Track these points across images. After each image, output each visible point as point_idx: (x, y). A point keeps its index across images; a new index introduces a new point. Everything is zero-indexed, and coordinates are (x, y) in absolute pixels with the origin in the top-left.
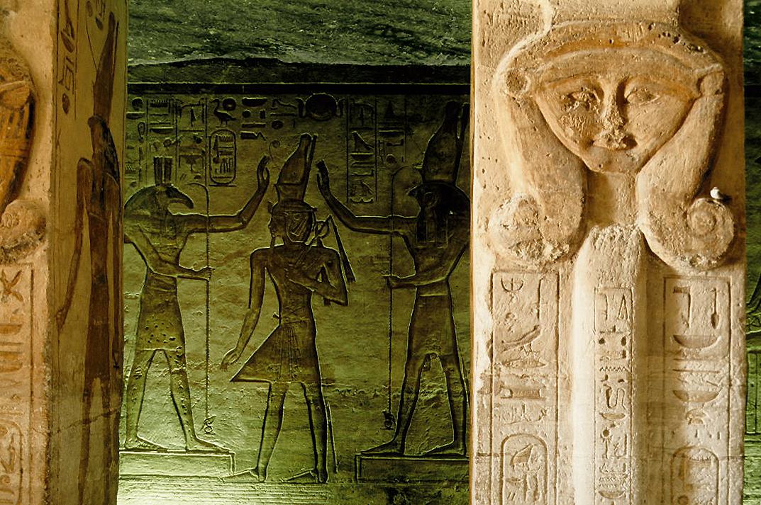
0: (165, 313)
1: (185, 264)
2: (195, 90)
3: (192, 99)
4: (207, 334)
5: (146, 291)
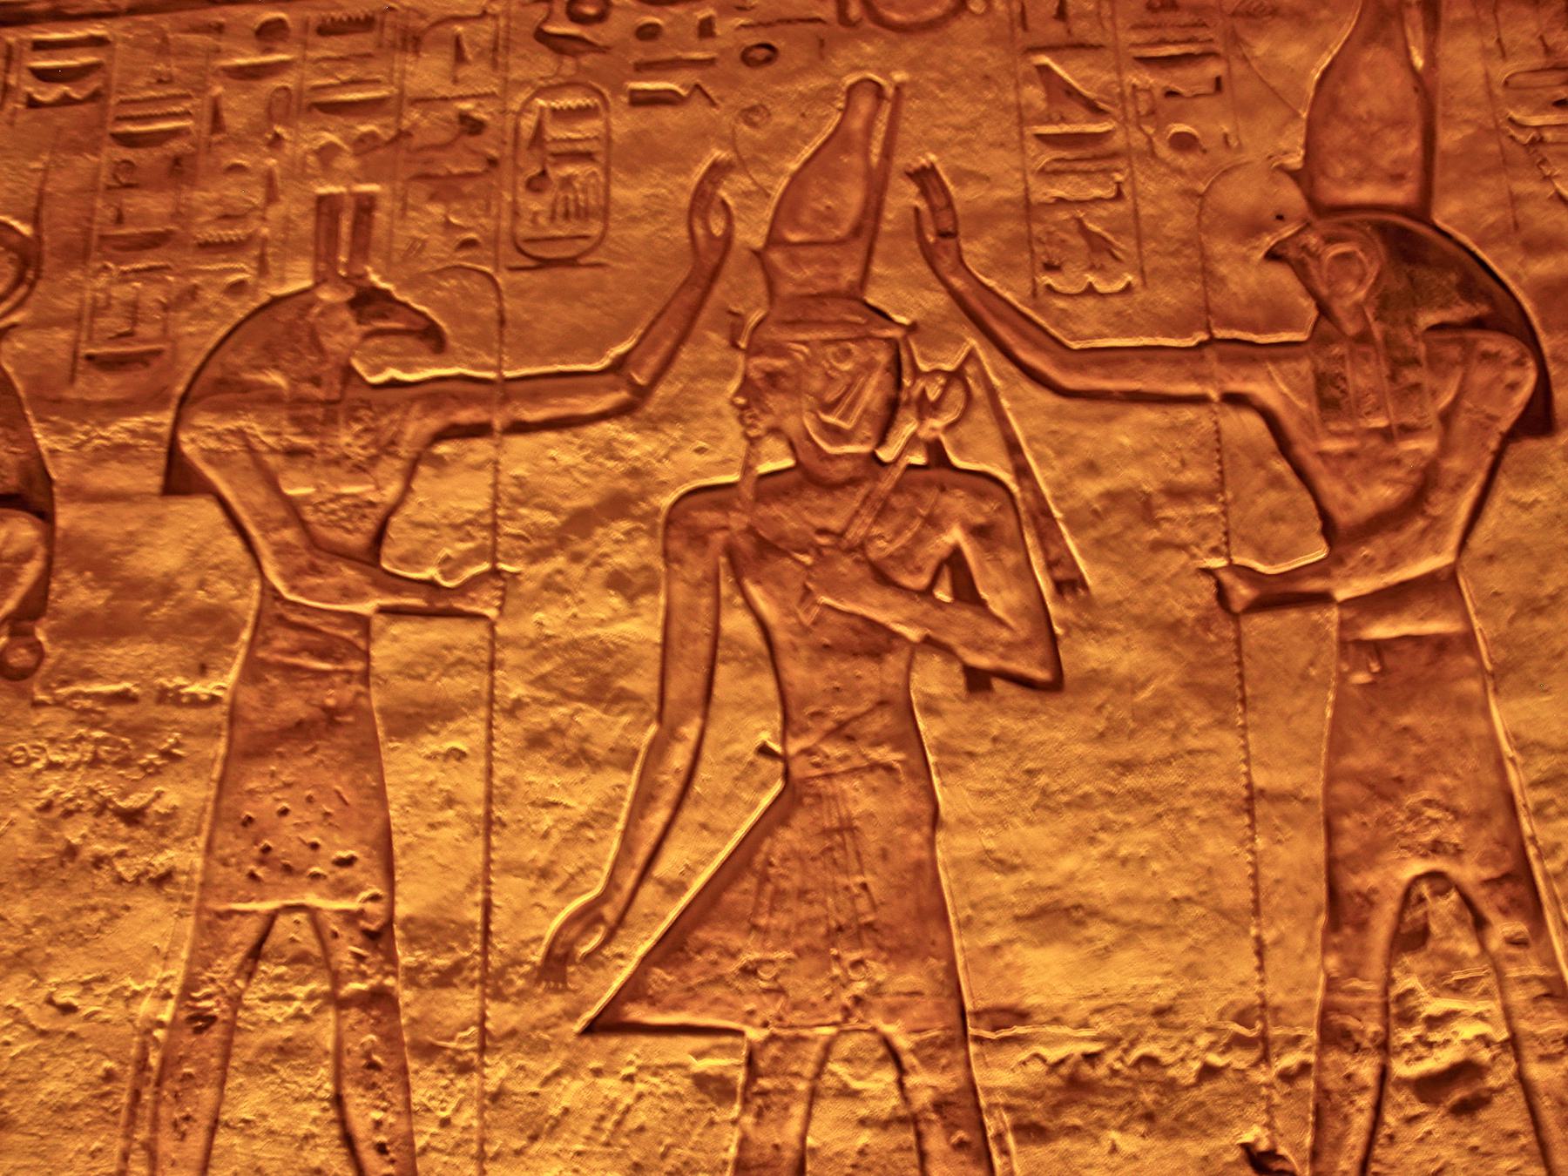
0: (317, 756)
1: (404, 560)
5: (254, 671)
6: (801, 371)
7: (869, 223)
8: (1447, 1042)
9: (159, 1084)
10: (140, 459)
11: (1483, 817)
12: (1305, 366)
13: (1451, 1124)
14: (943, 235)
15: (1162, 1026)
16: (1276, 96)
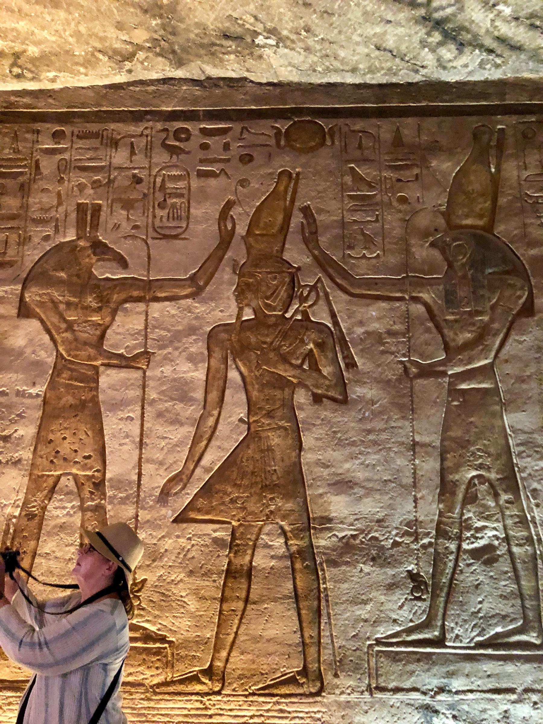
0: (78, 418)
2: (137, 117)
3: (133, 129)
4: (141, 449)
5: (52, 385)
6: (259, 283)
7: (286, 227)
8: (482, 538)
9: (13, 539)
10: (10, 303)
11: (498, 456)
12: (441, 287)
13: (483, 568)
14: (311, 233)
15: (379, 526)
16: (438, 182)
